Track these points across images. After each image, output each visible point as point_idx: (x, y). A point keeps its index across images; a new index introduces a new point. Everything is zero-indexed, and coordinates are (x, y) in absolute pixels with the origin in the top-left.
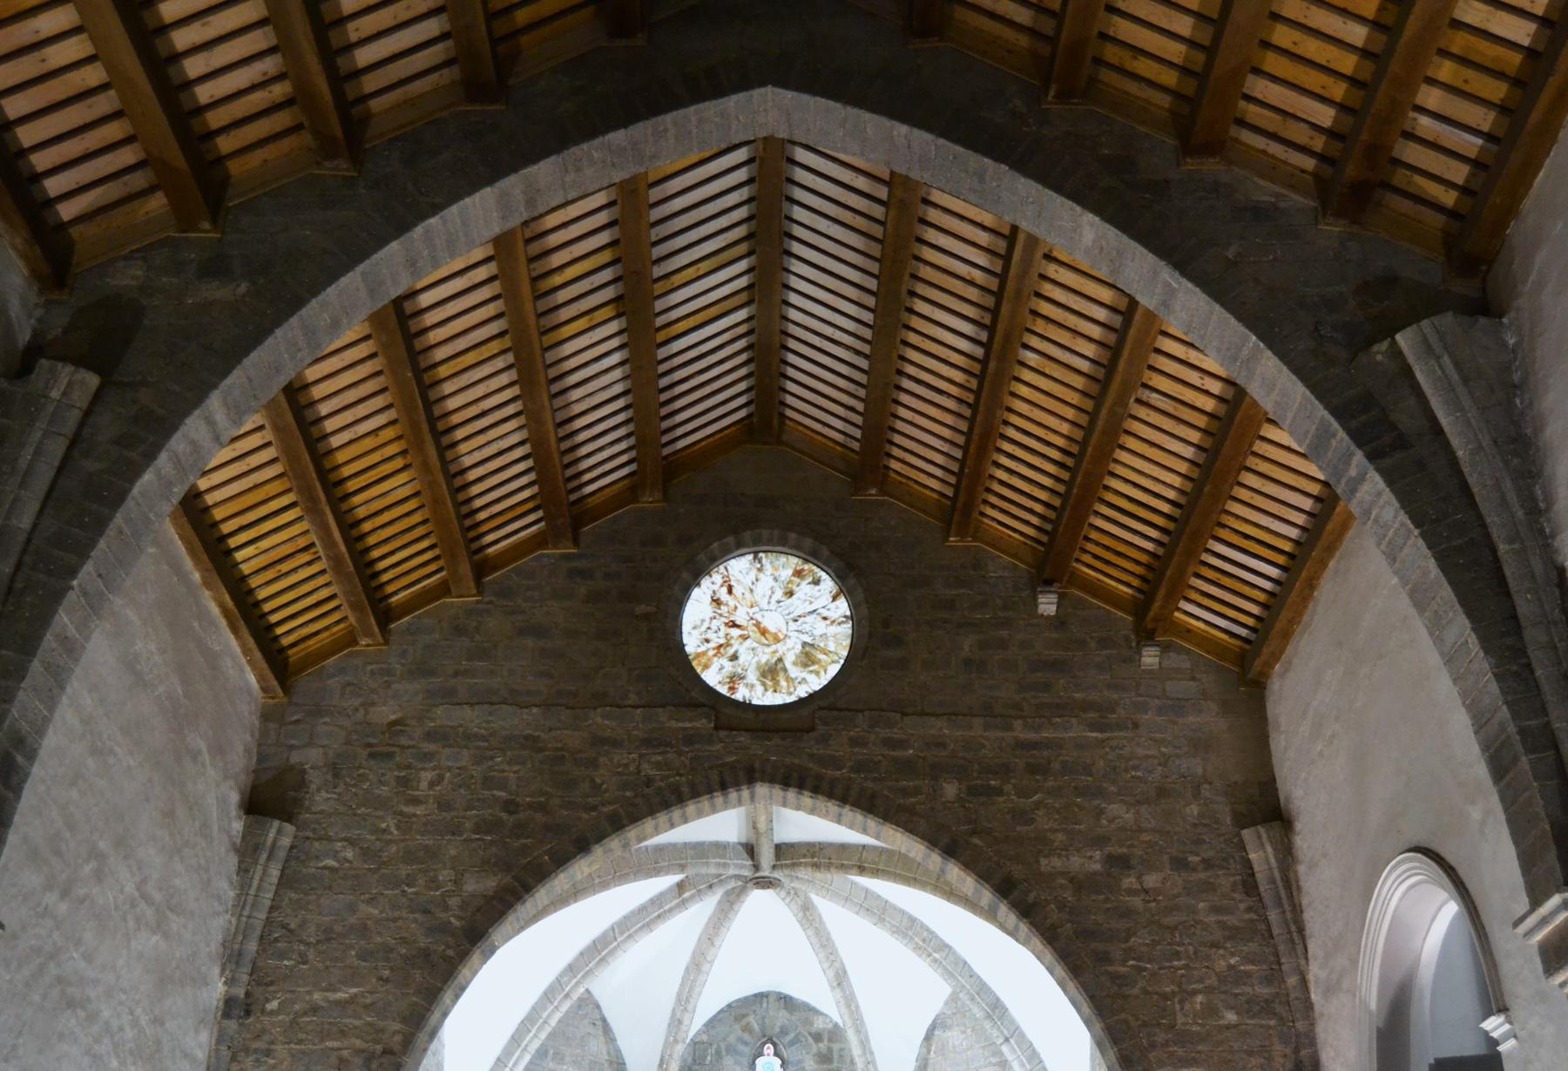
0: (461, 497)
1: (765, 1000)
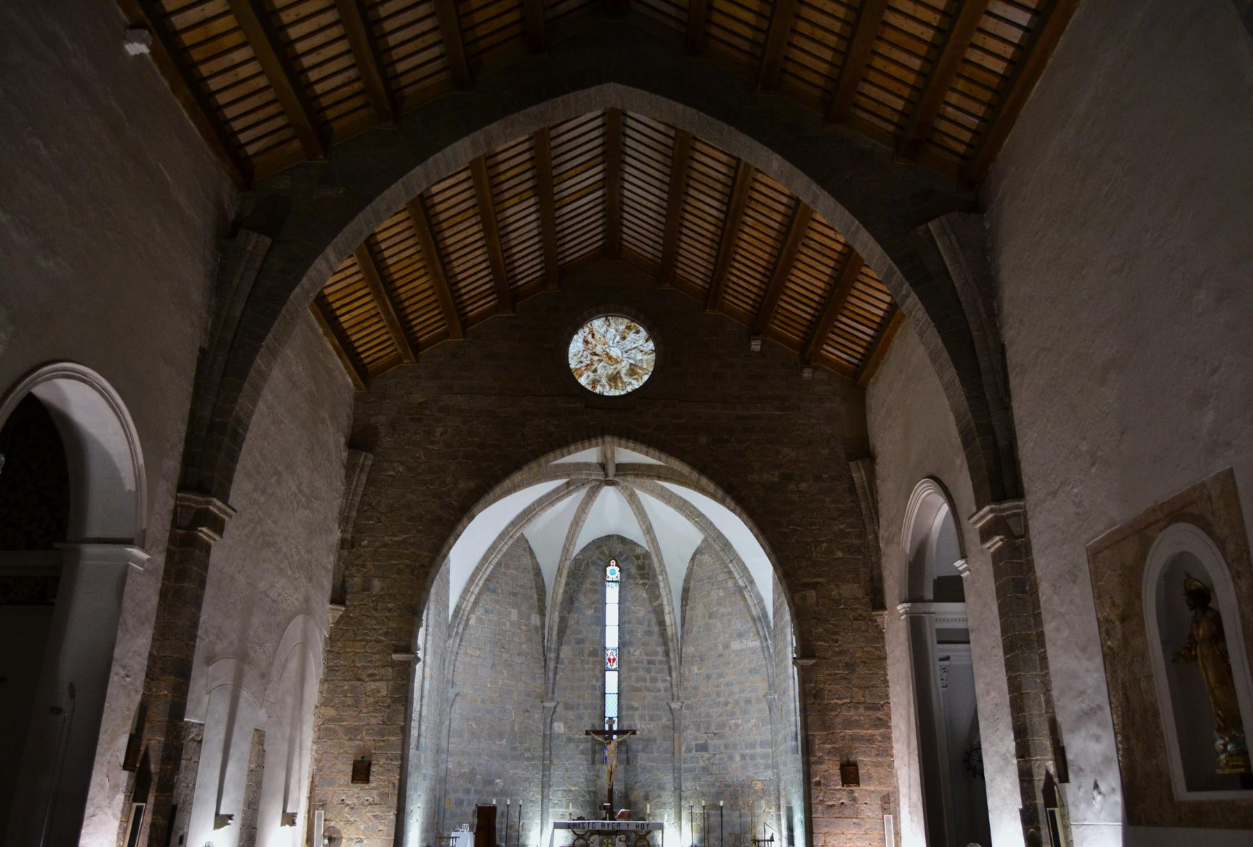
0: (454, 288)
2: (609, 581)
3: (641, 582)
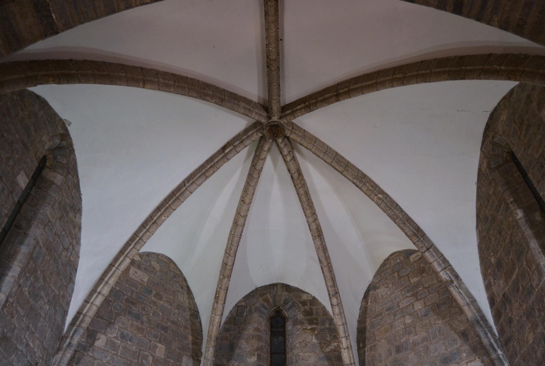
3: (309, 327)
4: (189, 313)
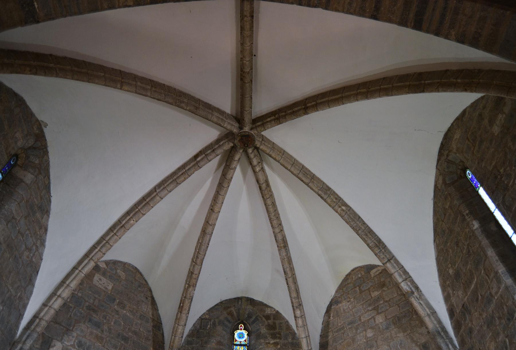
1: (240, 301)
2: (237, 345)
3: (272, 342)
4: (152, 324)
